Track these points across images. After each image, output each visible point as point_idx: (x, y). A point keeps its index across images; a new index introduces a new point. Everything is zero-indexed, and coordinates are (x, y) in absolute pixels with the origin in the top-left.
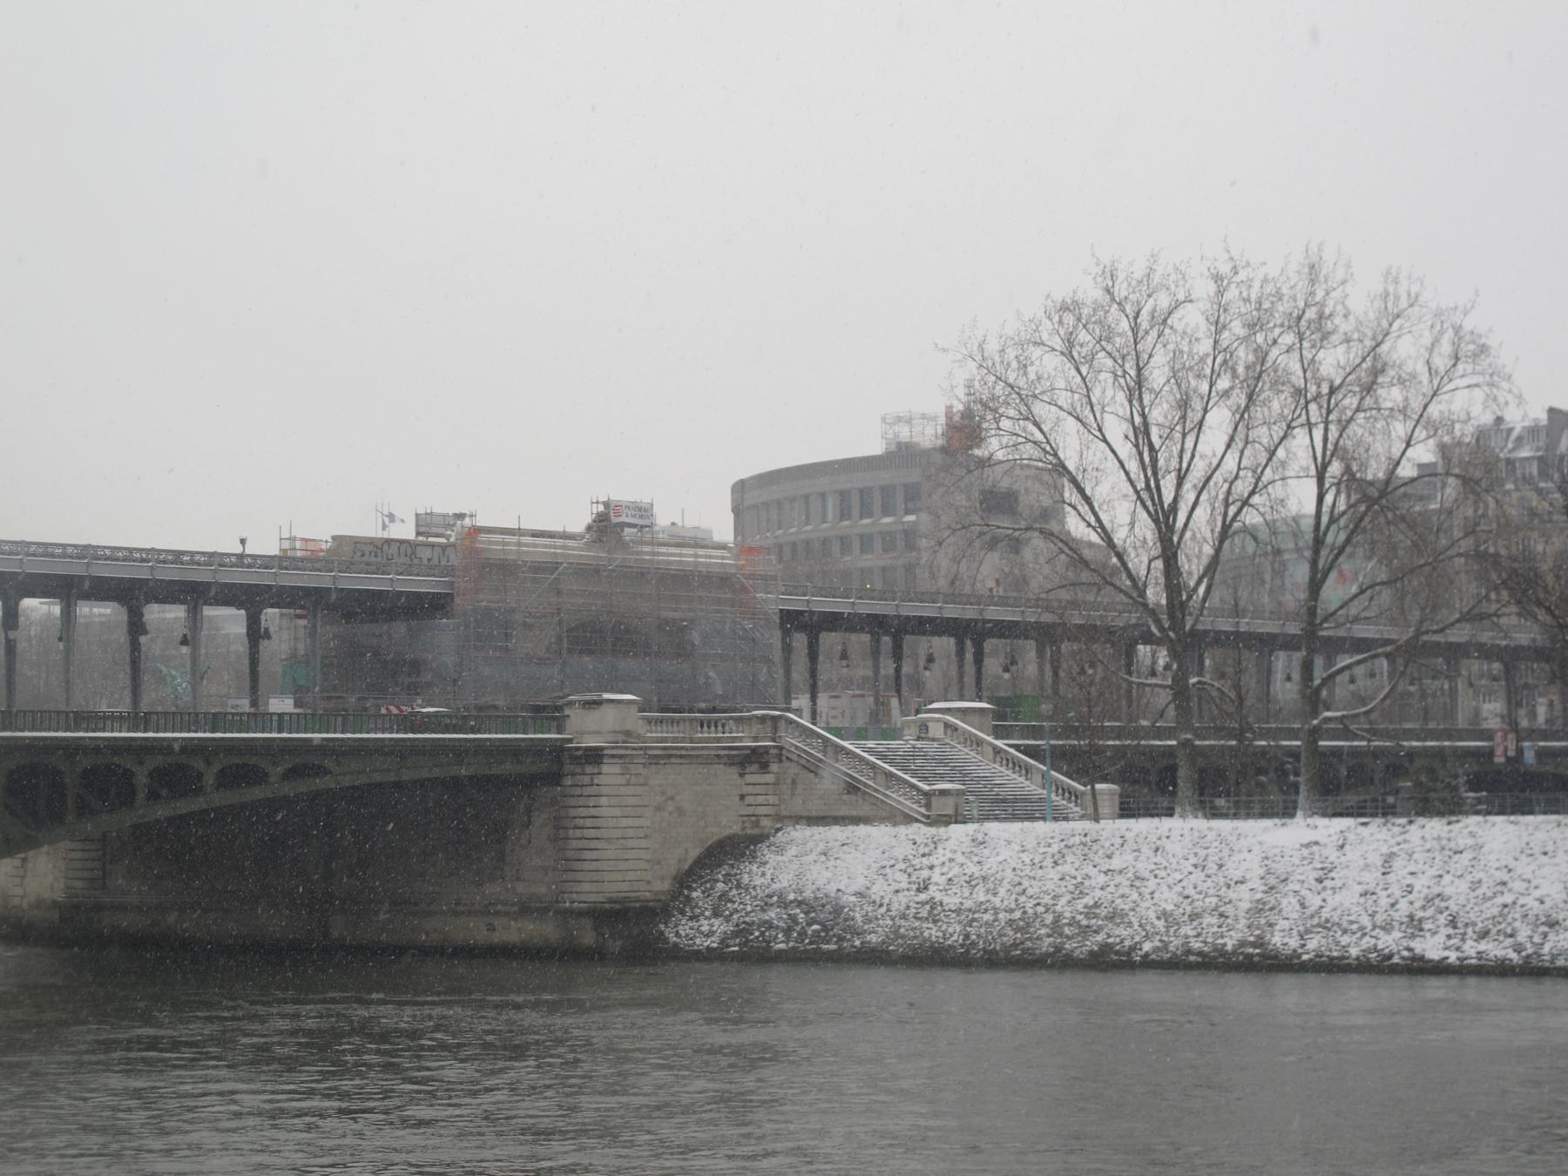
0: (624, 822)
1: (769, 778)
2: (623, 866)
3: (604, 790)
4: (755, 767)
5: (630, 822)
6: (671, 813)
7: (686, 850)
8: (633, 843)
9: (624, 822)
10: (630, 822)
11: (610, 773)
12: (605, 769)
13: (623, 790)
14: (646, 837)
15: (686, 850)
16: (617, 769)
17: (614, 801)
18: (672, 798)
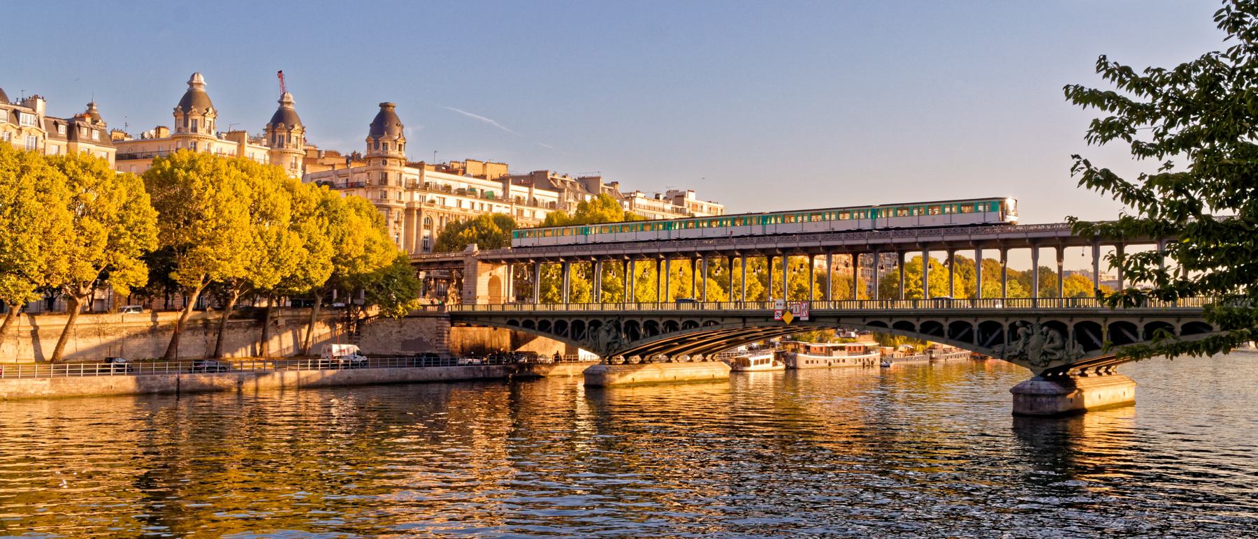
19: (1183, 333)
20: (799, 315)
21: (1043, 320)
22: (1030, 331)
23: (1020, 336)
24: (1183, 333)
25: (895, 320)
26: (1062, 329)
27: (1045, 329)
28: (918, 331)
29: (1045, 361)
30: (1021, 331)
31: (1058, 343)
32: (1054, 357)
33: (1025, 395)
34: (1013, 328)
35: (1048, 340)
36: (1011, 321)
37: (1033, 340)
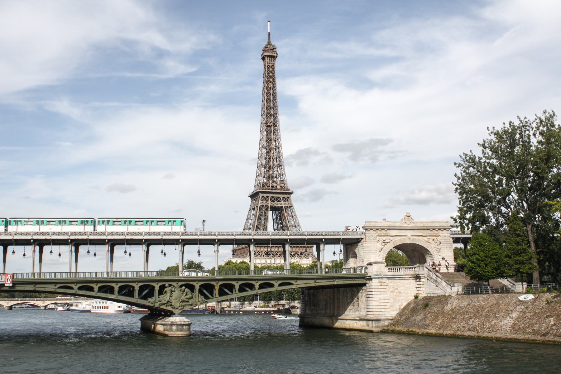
0: (380, 296)
1: (421, 283)
2: (380, 307)
3: (373, 287)
4: (418, 280)
5: (382, 295)
6: (396, 293)
7: (402, 303)
8: (382, 301)
9: (380, 296)
10: (382, 295)
11: (375, 282)
12: (373, 281)
13: (380, 287)
14: (388, 299)
15: (402, 303)
16: (378, 281)
17: (376, 290)
18: (397, 289)
19: (259, 289)
20: (4, 283)
21: (180, 283)
22: (173, 289)
23: (166, 292)
24: (259, 289)
25: (79, 285)
26: (192, 288)
27: (183, 288)
28: (96, 291)
29: (182, 306)
30: (168, 289)
31: (189, 296)
32: (188, 304)
33: (177, 325)
34: (162, 288)
35: (184, 295)
36: (161, 284)
37: (176, 294)
